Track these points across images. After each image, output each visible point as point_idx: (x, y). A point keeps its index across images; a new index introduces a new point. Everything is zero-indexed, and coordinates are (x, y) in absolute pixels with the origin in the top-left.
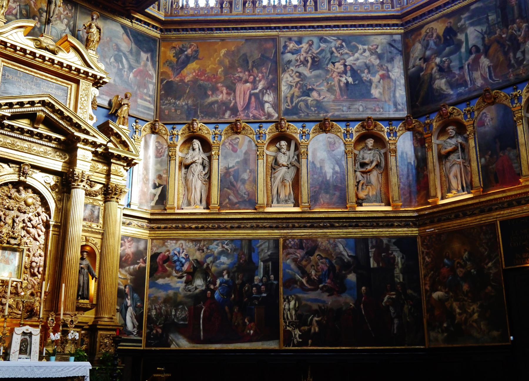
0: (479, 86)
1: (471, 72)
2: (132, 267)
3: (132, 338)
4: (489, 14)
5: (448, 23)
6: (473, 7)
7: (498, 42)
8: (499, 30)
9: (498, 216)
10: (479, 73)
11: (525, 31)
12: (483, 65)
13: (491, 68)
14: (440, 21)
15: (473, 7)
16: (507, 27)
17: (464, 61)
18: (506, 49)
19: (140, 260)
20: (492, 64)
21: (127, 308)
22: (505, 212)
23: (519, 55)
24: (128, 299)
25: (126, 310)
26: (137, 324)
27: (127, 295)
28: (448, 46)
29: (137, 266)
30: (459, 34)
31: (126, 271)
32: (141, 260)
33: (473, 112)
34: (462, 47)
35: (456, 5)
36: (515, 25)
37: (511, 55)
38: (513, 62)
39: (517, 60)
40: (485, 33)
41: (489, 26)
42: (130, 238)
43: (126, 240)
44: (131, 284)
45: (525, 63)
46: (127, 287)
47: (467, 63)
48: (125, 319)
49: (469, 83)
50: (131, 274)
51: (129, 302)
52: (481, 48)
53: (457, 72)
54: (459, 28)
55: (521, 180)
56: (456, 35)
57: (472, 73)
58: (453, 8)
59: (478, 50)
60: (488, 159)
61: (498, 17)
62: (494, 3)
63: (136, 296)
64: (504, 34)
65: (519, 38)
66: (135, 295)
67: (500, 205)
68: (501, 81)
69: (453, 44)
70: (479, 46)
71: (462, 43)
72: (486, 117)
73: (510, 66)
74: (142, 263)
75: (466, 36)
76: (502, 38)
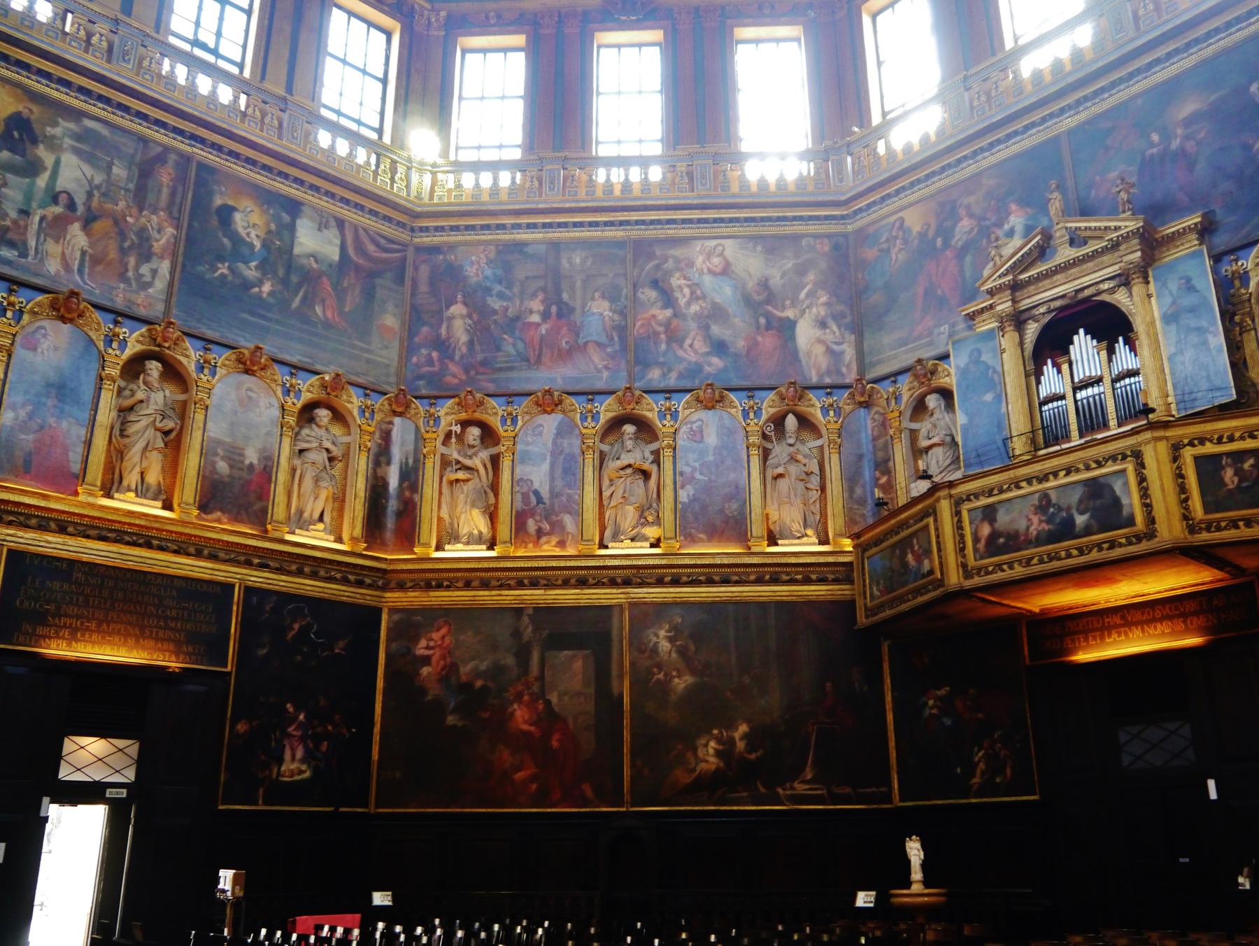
0: (53, 273)
1: (42, 236)
4: (115, 162)
5: (25, 107)
6: (89, 123)
7: (116, 223)
8: (124, 202)
9: (9, 538)
10: (60, 249)
11: (168, 241)
12: (73, 241)
13: (87, 258)
14: (7, 87)
15: (89, 123)
16: (141, 209)
17: (34, 205)
18: (127, 244)
20: (90, 250)
22: (28, 535)
23: (145, 269)
28: (10, 150)
30: (41, 147)
33: (21, 312)
34: (42, 176)
35: (57, 90)
36: (154, 217)
37: (132, 261)
38: (130, 274)
39: (139, 277)
40: (98, 187)
41: (108, 181)
45: (150, 290)
47: (40, 212)
49: (32, 252)
52: (81, 209)
53: (13, 214)
54: (46, 137)
55: (80, 490)
56: (35, 142)
57: (45, 240)
58: (47, 90)
59: (71, 206)
60: (21, 418)
61: (129, 179)
62: (131, 151)
64: (131, 216)
65: (154, 244)
67: (22, 519)
68: (97, 292)
69: (23, 156)
70: (76, 200)
71: (45, 169)
72: (44, 336)
73: (123, 277)
75: (57, 163)
76: (126, 221)
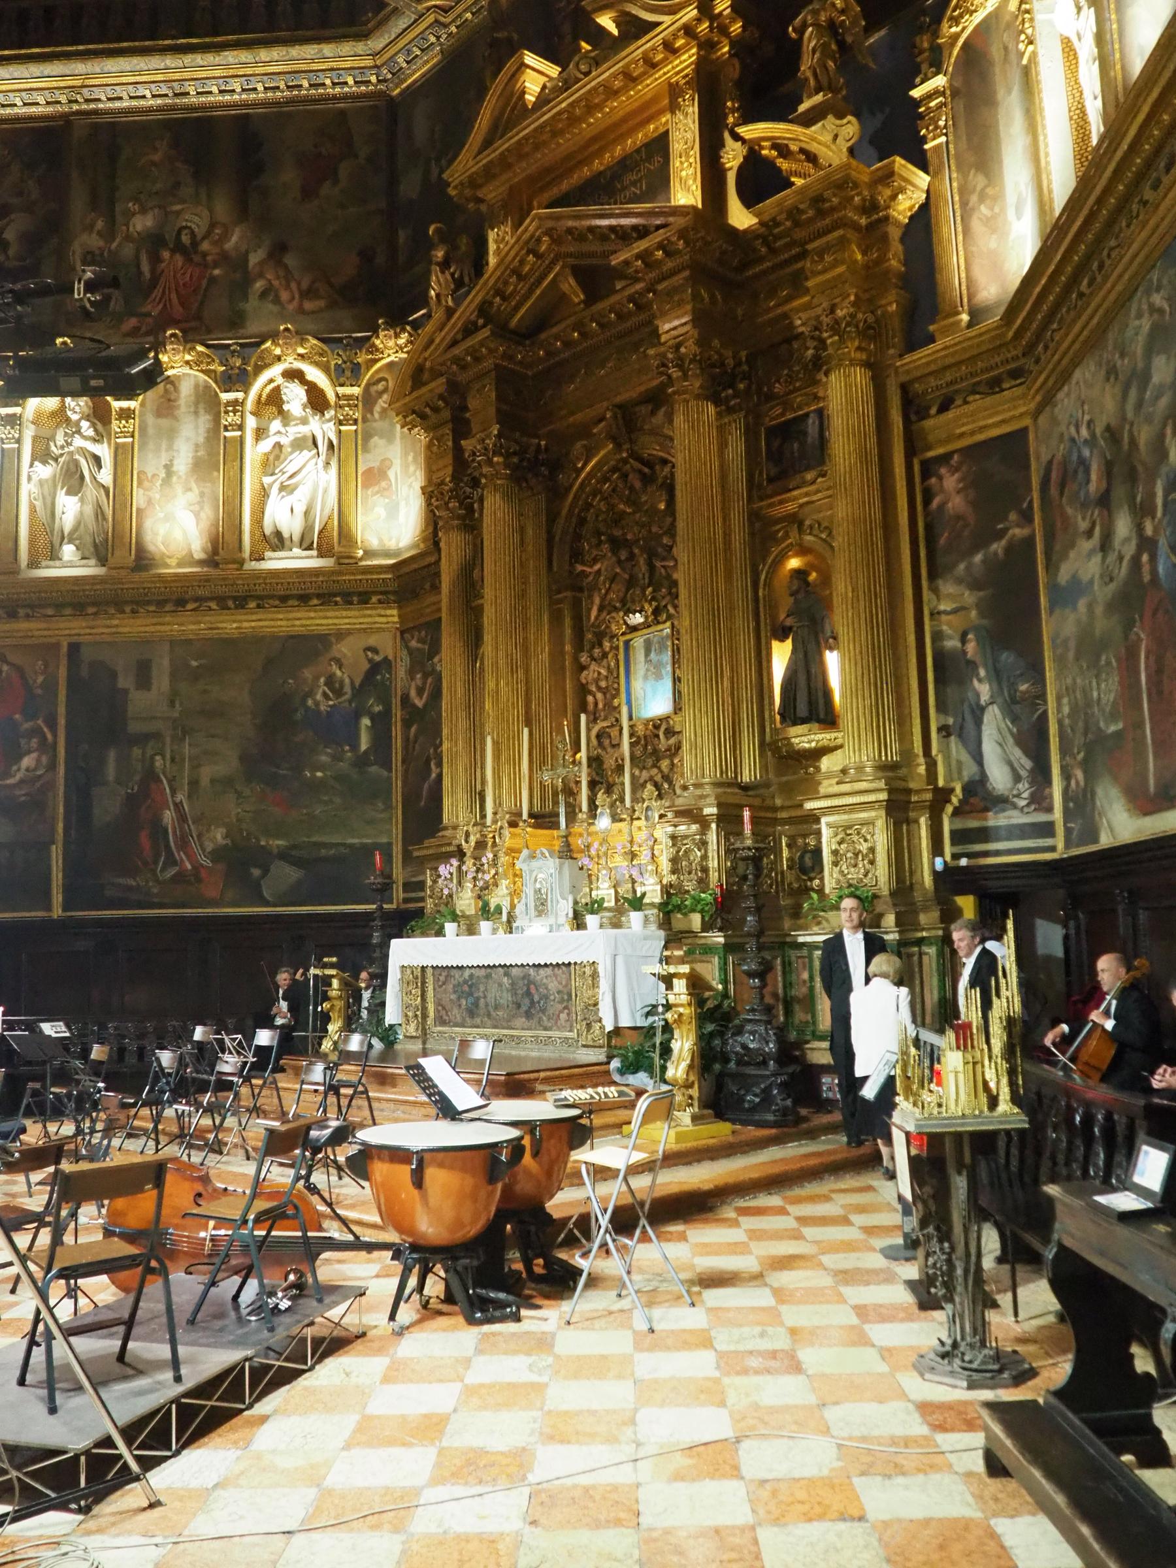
2: (978, 558)
3: (1015, 821)
19: (1005, 518)
21: (978, 712)
24: (980, 681)
25: (979, 723)
26: (1028, 764)
27: (972, 665)
29: (998, 547)
31: (959, 581)
32: (1013, 516)
42: (956, 457)
43: (943, 471)
44: (985, 622)
46: (970, 636)
48: (978, 758)
50: (975, 585)
51: (984, 690)
63: (1011, 659)
66: (1007, 658)
74: (1018, 526)
